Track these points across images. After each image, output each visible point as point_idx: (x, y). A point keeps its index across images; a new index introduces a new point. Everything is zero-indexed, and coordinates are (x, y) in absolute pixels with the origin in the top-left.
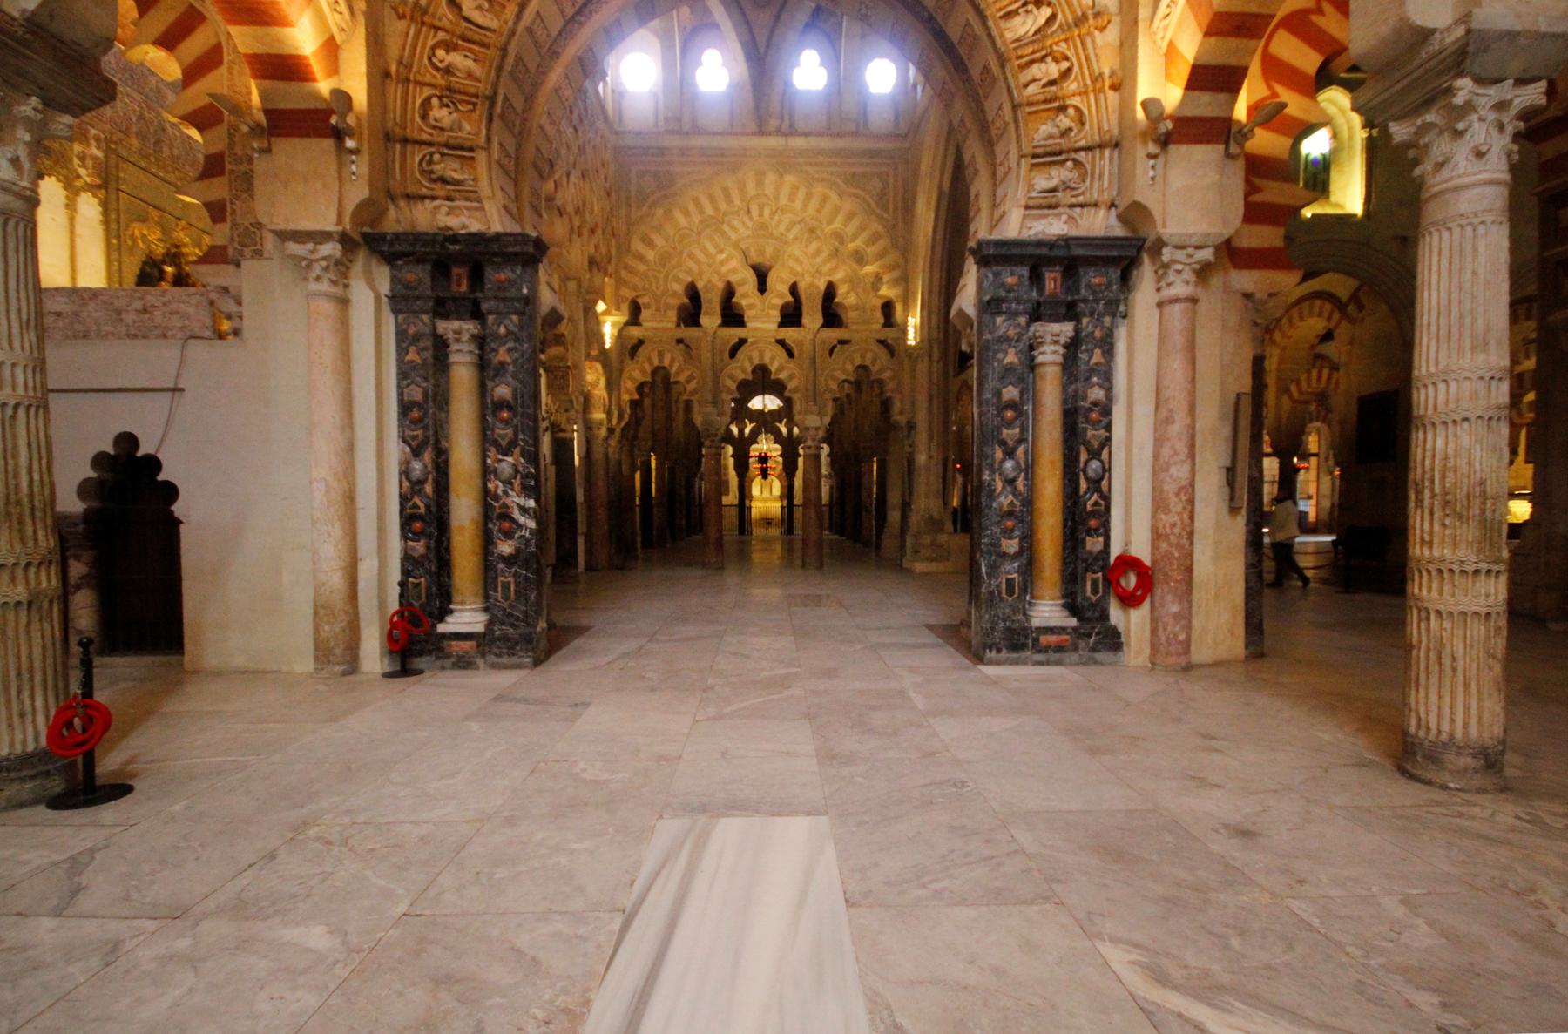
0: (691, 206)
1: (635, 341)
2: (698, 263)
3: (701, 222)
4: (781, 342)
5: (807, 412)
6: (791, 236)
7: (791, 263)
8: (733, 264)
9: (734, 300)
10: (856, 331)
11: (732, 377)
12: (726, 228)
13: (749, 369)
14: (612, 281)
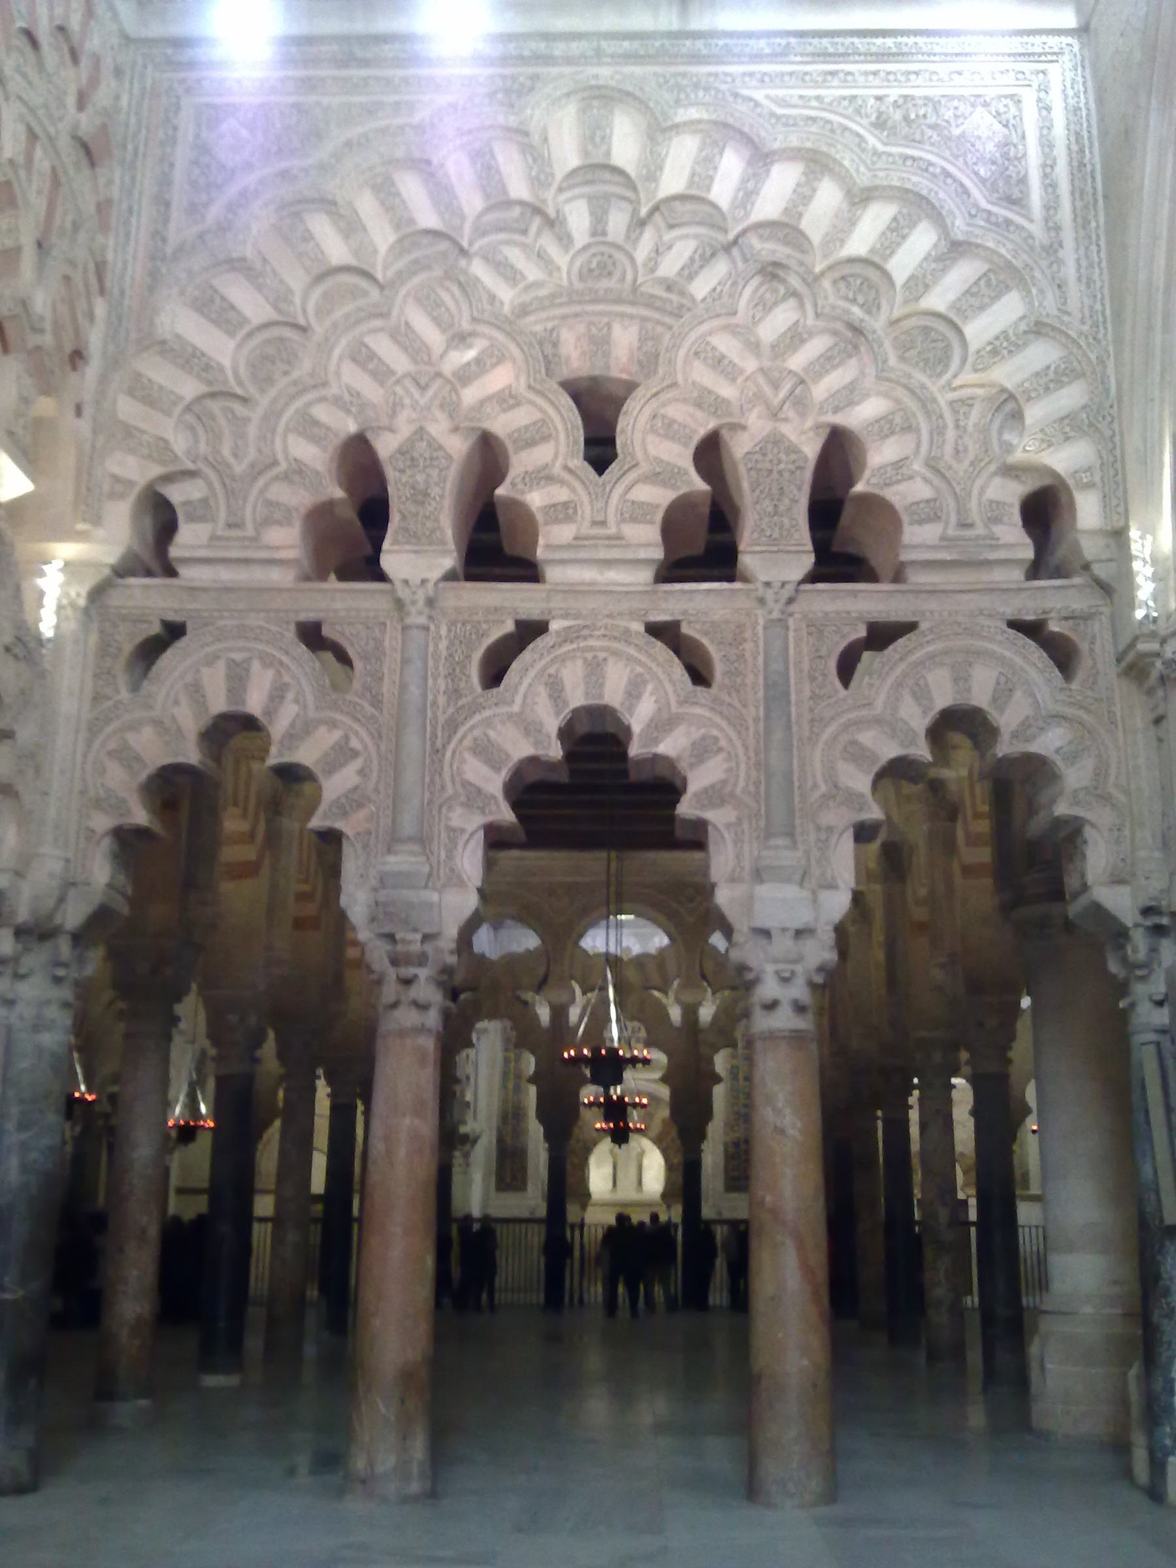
0: (367, 206)
1: (156, 629)
2: (381, 374)
5: (758, 875)
6: (701, 287)
7: (703, 375)
9: (500, 491)
11: (486, 751)
12: (478, 269)
13: (552, 724)
14: (84, 426)
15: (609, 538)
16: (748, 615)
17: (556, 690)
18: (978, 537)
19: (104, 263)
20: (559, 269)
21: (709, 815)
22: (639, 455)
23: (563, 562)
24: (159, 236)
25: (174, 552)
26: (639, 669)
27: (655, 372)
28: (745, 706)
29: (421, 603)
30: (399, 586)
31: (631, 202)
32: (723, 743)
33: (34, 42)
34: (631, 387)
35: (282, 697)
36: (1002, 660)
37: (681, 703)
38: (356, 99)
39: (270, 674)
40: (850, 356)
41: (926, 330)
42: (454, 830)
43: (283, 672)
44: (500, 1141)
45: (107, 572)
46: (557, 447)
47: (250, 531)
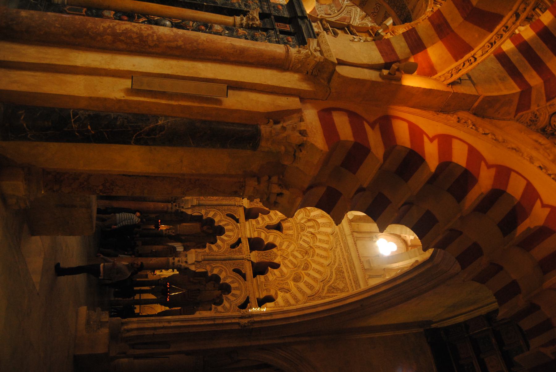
4: (239, 241)
5: (197, 255)
7: (286, 244)
9: (260, 214)
11: (215, 215)
13: (221, 224)
15: (254, 229)
16: (244, 254)
17: (227, 225)
21: (207, 248)
23: (249, 223)
26: (232, 237)
29: (239, 204)
32: (220, 250)
36: (241, 295)
40: (294, 266)
41: (300, 278)
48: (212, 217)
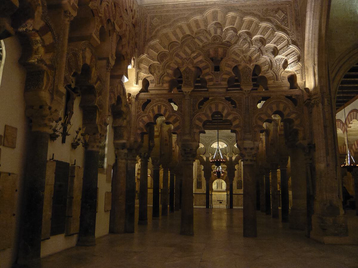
0: (178, 31)
2: (181, 58)
3: (183, 38)
4: (228, 99)
5: (244, 139)
8: (200, 58)
10: (273, 92)
11: (200, 120)
12: (196, 40)
13: (210, 115)
15: (219, 84)
18: (280, 82)
19: (137, 43)
20: (209, 40)
22: (224, 70)
24: (145, 38)
25: (149, 88)
27: (226, 56)
28: (242, 111)
30: (184, 93)
31: (221, 28)
32: (238, 117)
33: (127, 11)
34: (222, 59)
35: (166, 111)
37: (231, 111)
38: (176, 13)
39: (164, 107)
42: (195, 132)
43: (166, 107)
44: (197, 180)
45: (139, 92)
46: (210, 70)
47: (161, 85)
48: (201, 122)
